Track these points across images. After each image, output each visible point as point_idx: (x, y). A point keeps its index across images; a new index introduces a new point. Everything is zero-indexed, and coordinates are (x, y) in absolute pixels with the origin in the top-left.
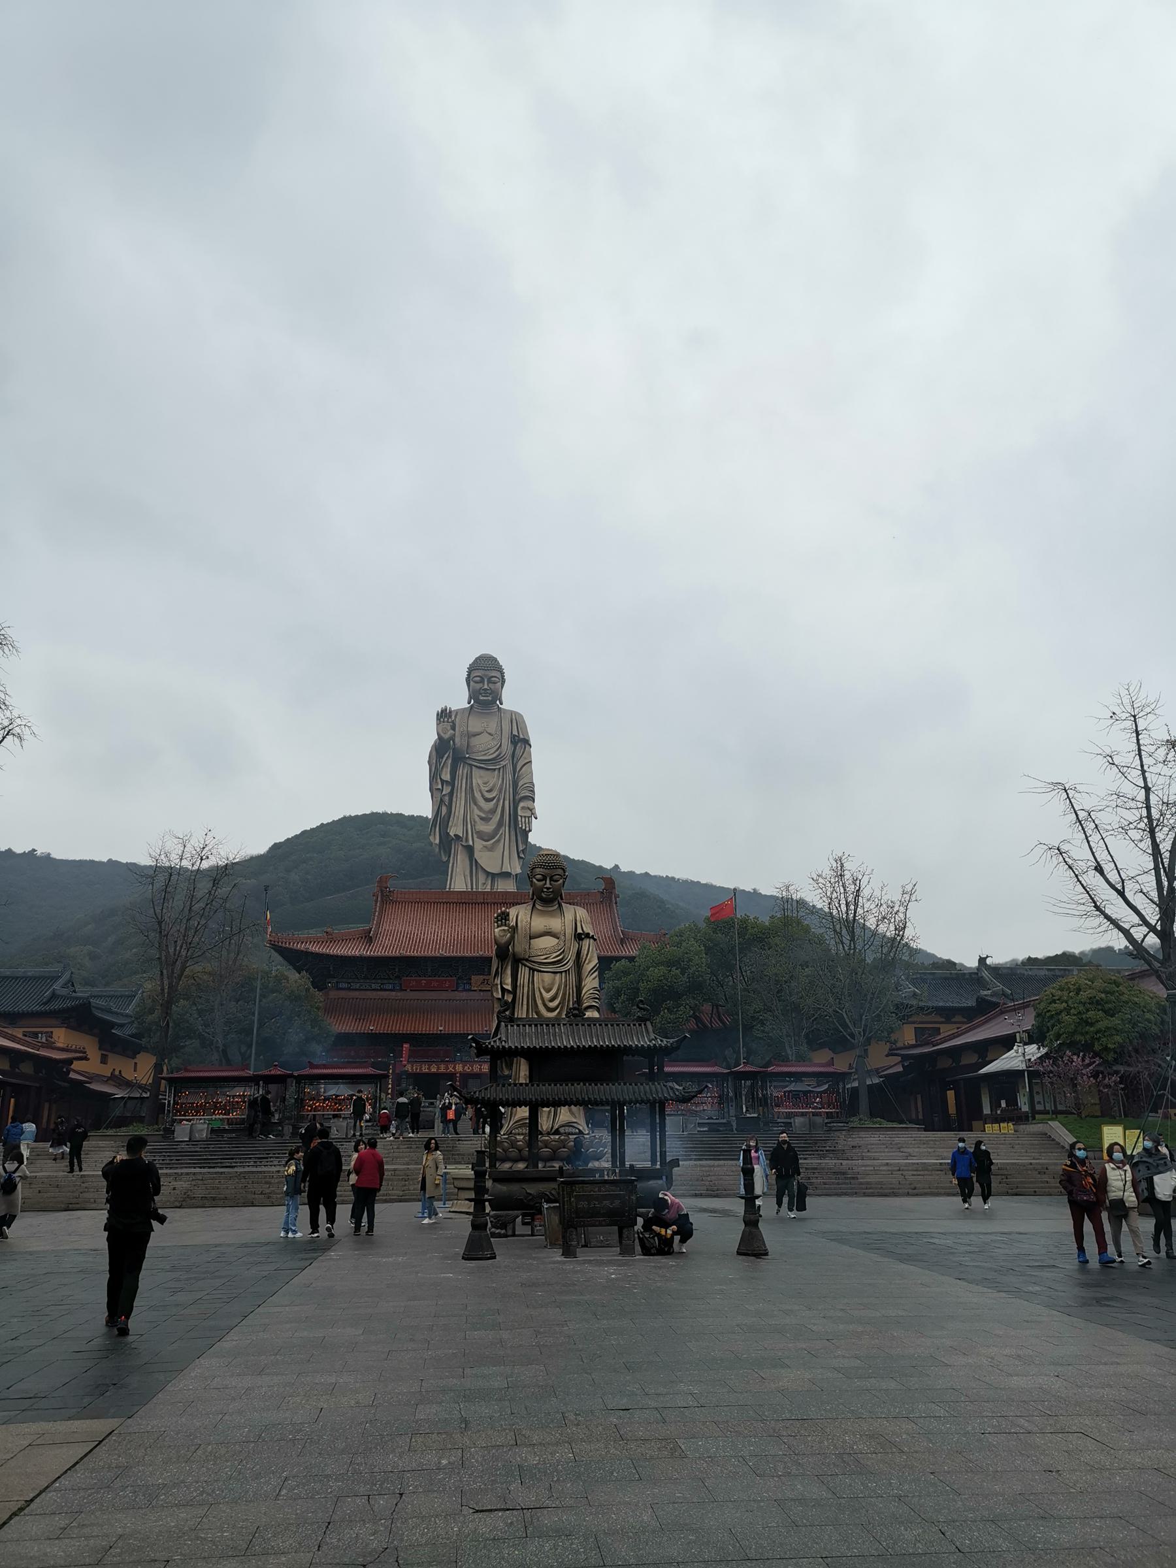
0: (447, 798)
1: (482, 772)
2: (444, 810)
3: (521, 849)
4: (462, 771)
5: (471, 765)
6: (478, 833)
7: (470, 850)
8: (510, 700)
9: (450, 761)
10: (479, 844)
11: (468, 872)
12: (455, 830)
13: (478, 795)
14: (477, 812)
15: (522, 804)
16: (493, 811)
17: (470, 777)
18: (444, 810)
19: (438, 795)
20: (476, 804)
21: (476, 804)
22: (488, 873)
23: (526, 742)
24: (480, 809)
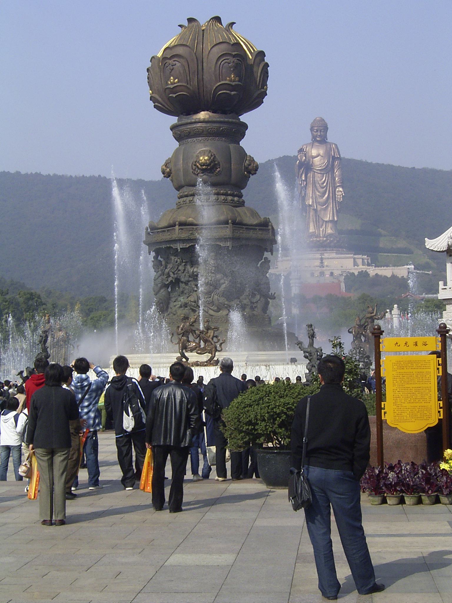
4: (310, 175)
5: (315, 172)
7: (316, 210)
8: (331, 137)
10: (319, 207)
13: (318, 185)
14: (317, 193)
15: (337, 190)
17: (314, 177)
18: (303, 192)
20: (317, 190)
21: (317, 190)
24: (319, 192)
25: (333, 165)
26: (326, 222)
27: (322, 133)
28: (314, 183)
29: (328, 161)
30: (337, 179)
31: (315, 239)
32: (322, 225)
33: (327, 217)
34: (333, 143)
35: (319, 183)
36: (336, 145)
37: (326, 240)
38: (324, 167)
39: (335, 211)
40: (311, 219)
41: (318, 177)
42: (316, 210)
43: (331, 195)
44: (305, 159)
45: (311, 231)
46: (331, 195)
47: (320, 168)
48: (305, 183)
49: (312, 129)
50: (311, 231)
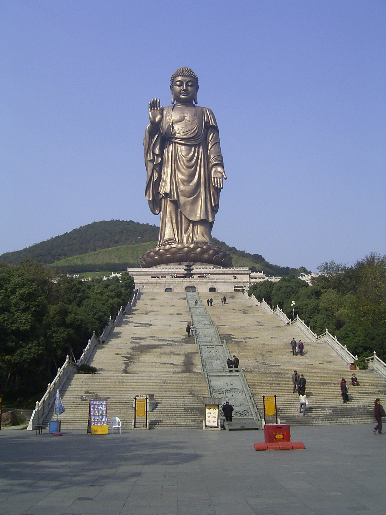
0: (158, 169)
1: (183, 147)
2: (156, 175)
3: (213, 204)
5: (176, 143)
6: (181, 191)
8: (203, 99)
9: (159, 139)
10: (182, 199)
11: (174, 221)
12: (165, 188)
14: (180, 176)
15: (214, 170)
16: (192, 176)
18: (156, 175)
19: (150, 165)
21: (179, 170)
22: (190, 221)
23: (215, 129)
24: (182, 174)
25: (206, 137)
26: (195, 223)
27: (189, 88)
28: (175, 160)
29: (200, 127)
30: (212, 157)
31: (173, 246)
32: (187, 229)
33: (196, 215)
34: (206, 108)
35: (183, 161)
36: (211, 112)
37: (194, 249)
38: (192, 136)
39: (209, 207)
40: (168, 219)
41: (182, 150)
42: (176, 203)
43: (202, 180)
44: (161, 120)
45: (166, 237)
46: (202, 180)
47: (185, 137)
48: (160, 159)
49: (173, 81)
50: (166, 237)
